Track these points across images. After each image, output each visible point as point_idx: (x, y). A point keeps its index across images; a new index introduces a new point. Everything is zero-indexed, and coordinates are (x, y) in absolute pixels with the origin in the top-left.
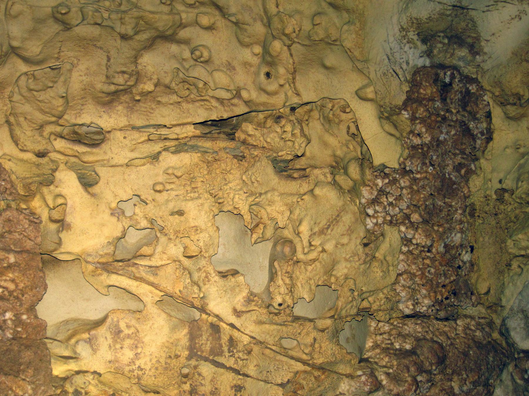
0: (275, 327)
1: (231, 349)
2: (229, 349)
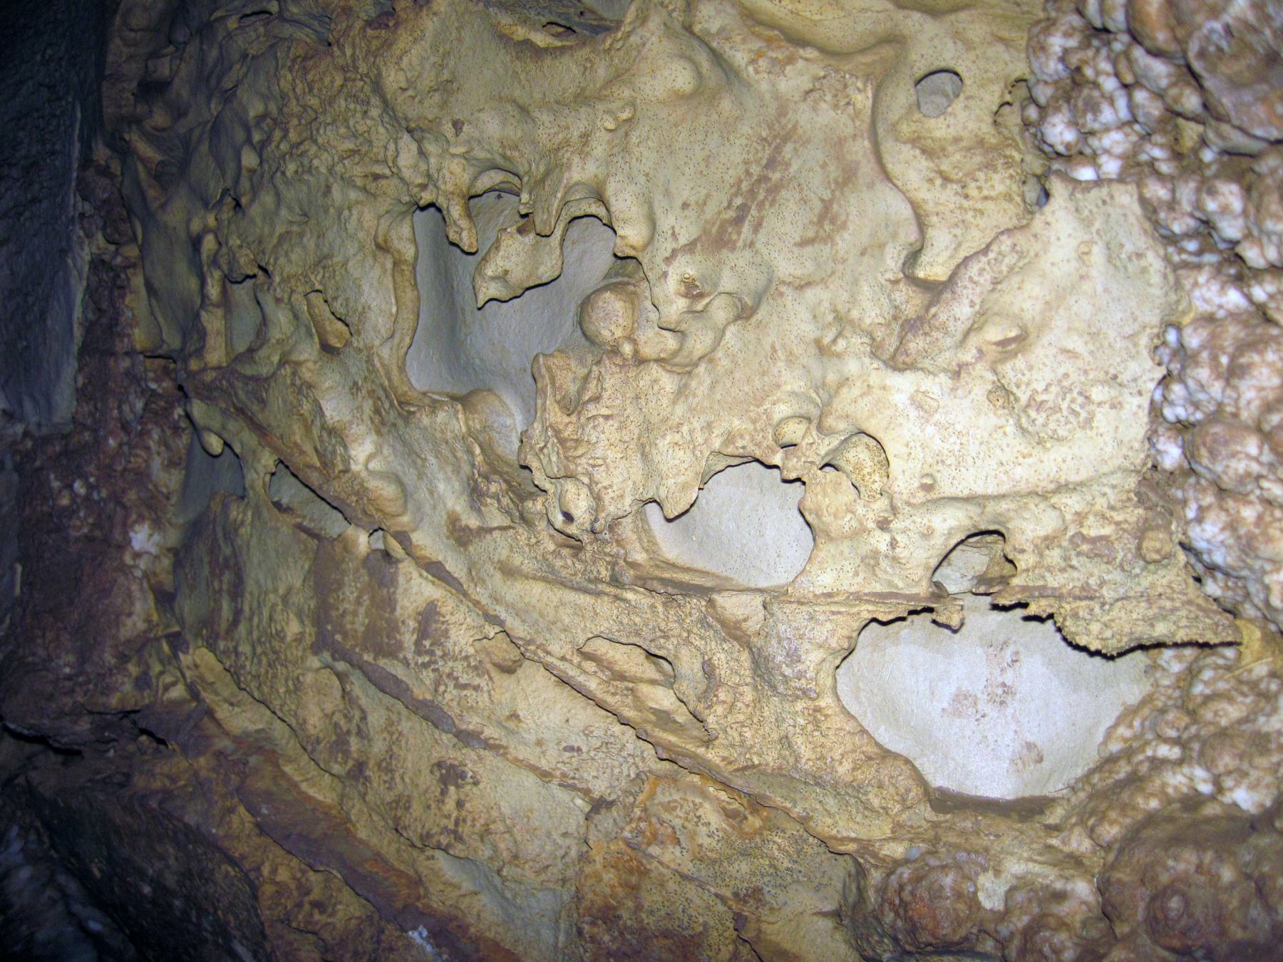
0: (571, 596)
1: (427, 643)
2: (418, 643)
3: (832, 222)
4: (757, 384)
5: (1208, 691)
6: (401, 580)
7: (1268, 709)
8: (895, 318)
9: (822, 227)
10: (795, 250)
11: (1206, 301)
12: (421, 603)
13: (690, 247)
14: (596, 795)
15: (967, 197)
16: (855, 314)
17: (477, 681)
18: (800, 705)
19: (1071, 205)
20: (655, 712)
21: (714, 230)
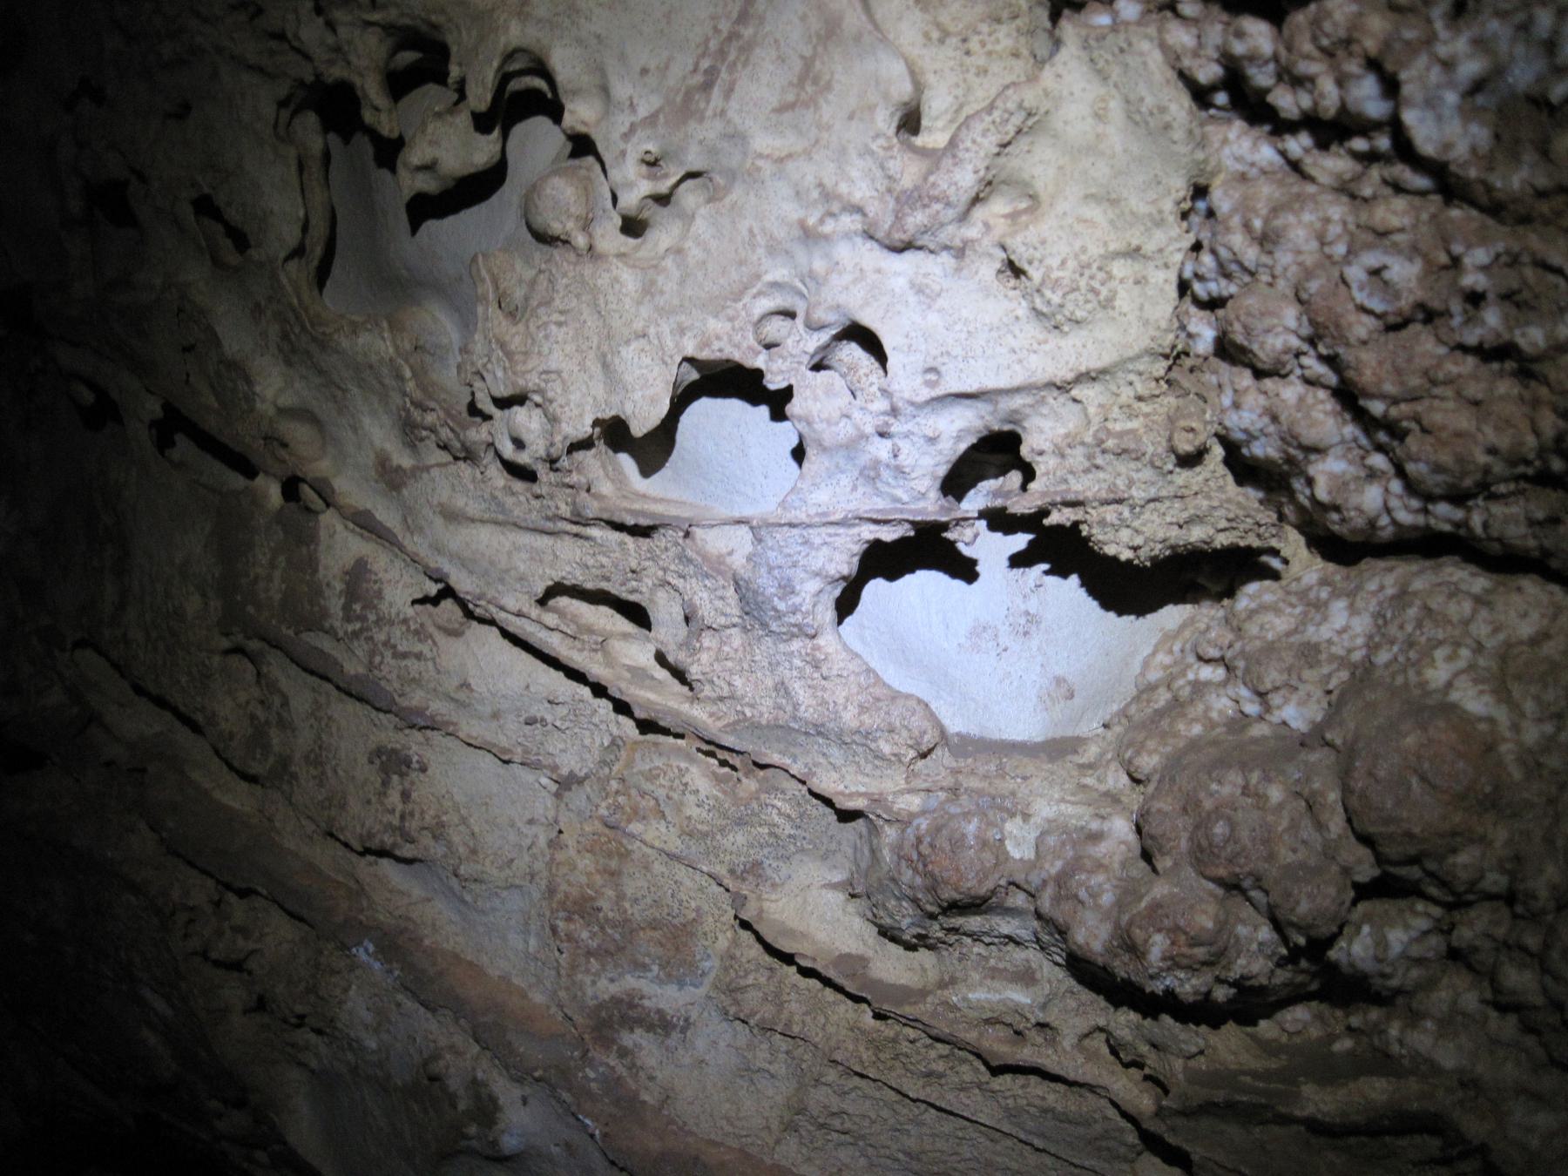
1: (357, 607)
2: (347, 608)
3: (815, 81)
4: (734, 275)
5: (1253, 605)
6: (323, 534)
7: (1318, 617)
8: (889, 191)
9: (803, 88)
10: (774, 117)
11: (1238, 159)
12: (348, 561)
13: (651, 120)
14: (565, 771)
15: (968, 53)
16: (843, 188)
17: (418, 647)
18: (796, 645)
19: (1084, 55)
20: (630, 669)
21: (679, 99)
